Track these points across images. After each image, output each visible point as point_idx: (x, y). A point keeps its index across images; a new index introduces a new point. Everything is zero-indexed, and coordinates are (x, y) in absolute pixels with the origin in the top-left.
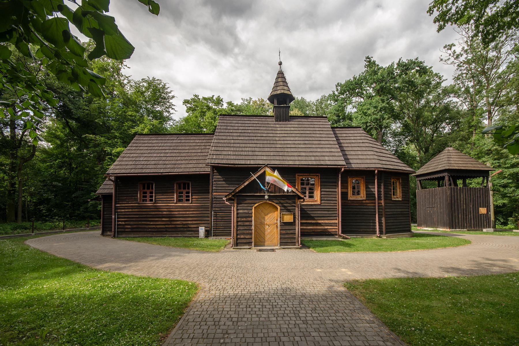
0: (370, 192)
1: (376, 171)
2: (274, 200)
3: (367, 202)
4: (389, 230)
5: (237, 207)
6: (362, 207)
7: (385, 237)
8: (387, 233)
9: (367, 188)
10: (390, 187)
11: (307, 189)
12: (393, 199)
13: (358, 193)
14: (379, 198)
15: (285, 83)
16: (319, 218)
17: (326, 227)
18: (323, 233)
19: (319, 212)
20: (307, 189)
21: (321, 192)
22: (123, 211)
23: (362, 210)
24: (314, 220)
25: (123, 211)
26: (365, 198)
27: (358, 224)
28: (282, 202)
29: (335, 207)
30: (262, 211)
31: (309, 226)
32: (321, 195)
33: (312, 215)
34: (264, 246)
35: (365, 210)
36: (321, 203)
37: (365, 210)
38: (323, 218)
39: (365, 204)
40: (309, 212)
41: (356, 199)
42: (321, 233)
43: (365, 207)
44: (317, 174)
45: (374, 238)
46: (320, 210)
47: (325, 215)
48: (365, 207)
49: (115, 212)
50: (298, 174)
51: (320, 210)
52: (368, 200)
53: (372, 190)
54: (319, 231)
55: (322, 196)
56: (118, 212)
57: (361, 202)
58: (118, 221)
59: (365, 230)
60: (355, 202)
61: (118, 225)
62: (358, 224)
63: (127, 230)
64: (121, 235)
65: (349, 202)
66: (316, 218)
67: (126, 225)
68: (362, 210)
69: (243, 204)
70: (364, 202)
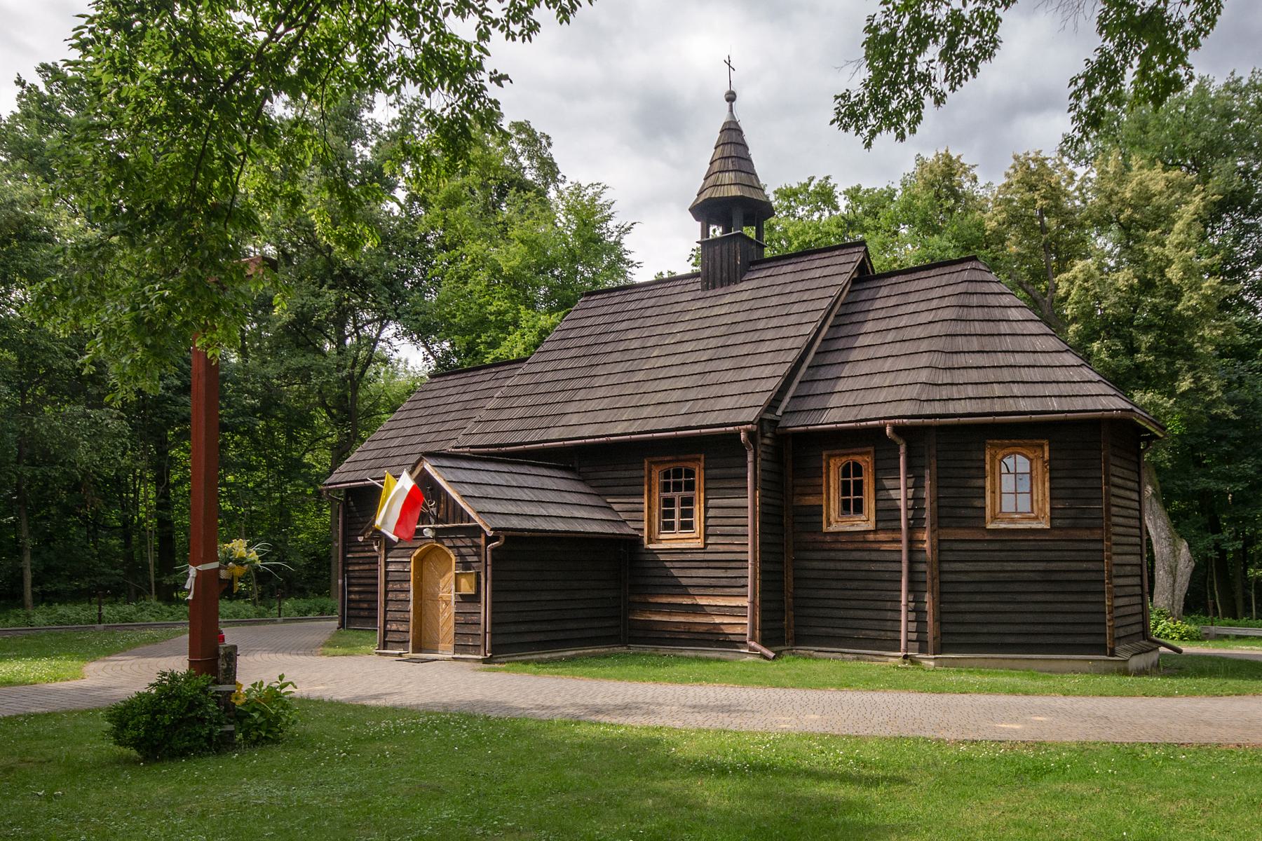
0: (889, 503)
1: (743, 436)
2: (445, 541)
3: (881, 536)
4: (947, 640)
5: (386, 558)
6: (866, 556)
7: (932, 663)
8: (942, 648)
9: (879, 488)
10: (979, 483)
11: (677, 501)
12: (990, 526)
13: (859, 508)
14: (915, 524)
15: (740, 148)
16: (702, 591)
17: (718, 620)
18: (710, 637)
19: (701, 573)
20: (677, 501)
21: (706, 512)
22: (357, 568)
23: (865, 566)
24: (689, 595)
25: (357, 568)
26: (871, 526)
27: (851, 613)
28: (459, 543)
29: (742, 557)
30: (435, 568)
31: (677, 614)
32: (706, 518)
33: (684, 582)
34: (435, 651)
35: (873, 567)
36: (706, 545)
37: (873, 567)
38: (710, 591)
39: (875, 546)
40: (675, 573)
41: (852, 529)
42: (706, 637)
43: (874, 556)
44: (698, 456)
45: (894, 659)
46: (704, 565)
47: (714, 582)
48: (874, 556)
49: (344, 571)
50: (651, 459)
51: (704, 565)
52: (885, 530)
53: (893, 494)
54: (702, 629)
55: (710, 522)
56: (348, 571)
57: (860, 538)
58: (350, 593)
59: (873, 634)
60: (843, 538)
61: (349, 600)
62: (851, 613)
63: (362, 613)
64: (354, 625)
65: (828, 539)
66: (691, 591)
67: (360, 601)
68: (865, 566)
69: (396, 551)
70: (871, 537)
